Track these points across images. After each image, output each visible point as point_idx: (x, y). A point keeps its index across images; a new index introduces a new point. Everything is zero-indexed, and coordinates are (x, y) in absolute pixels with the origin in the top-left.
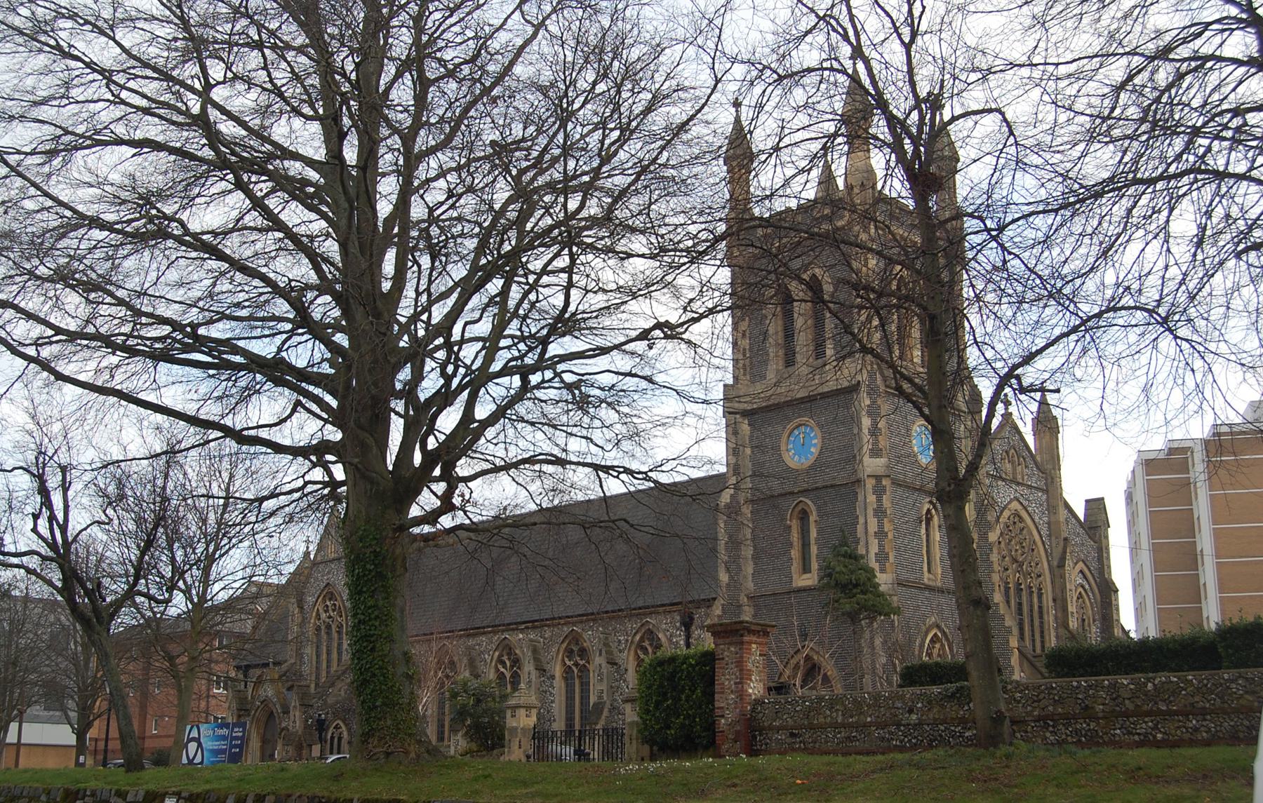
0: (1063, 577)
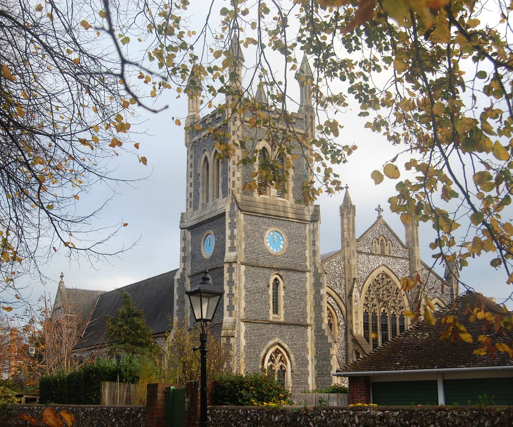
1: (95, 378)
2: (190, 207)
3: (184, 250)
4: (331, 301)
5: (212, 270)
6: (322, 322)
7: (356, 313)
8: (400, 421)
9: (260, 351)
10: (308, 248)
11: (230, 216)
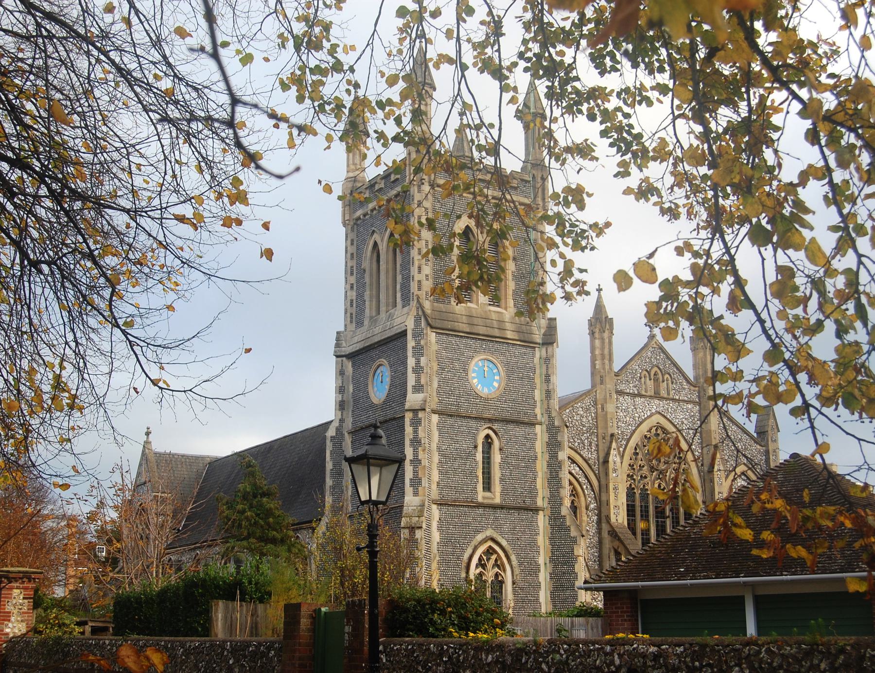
0: (712, 481)
1: (202, 595)
2: (351, 322)
3: (341, 390)
4: (576, 470)
5: (386, 421)
6: (561, 504)
7: (615, 489)
8: (685, 662)
9: (463, 550)
10: (538, 386)
11: (414, 336)
